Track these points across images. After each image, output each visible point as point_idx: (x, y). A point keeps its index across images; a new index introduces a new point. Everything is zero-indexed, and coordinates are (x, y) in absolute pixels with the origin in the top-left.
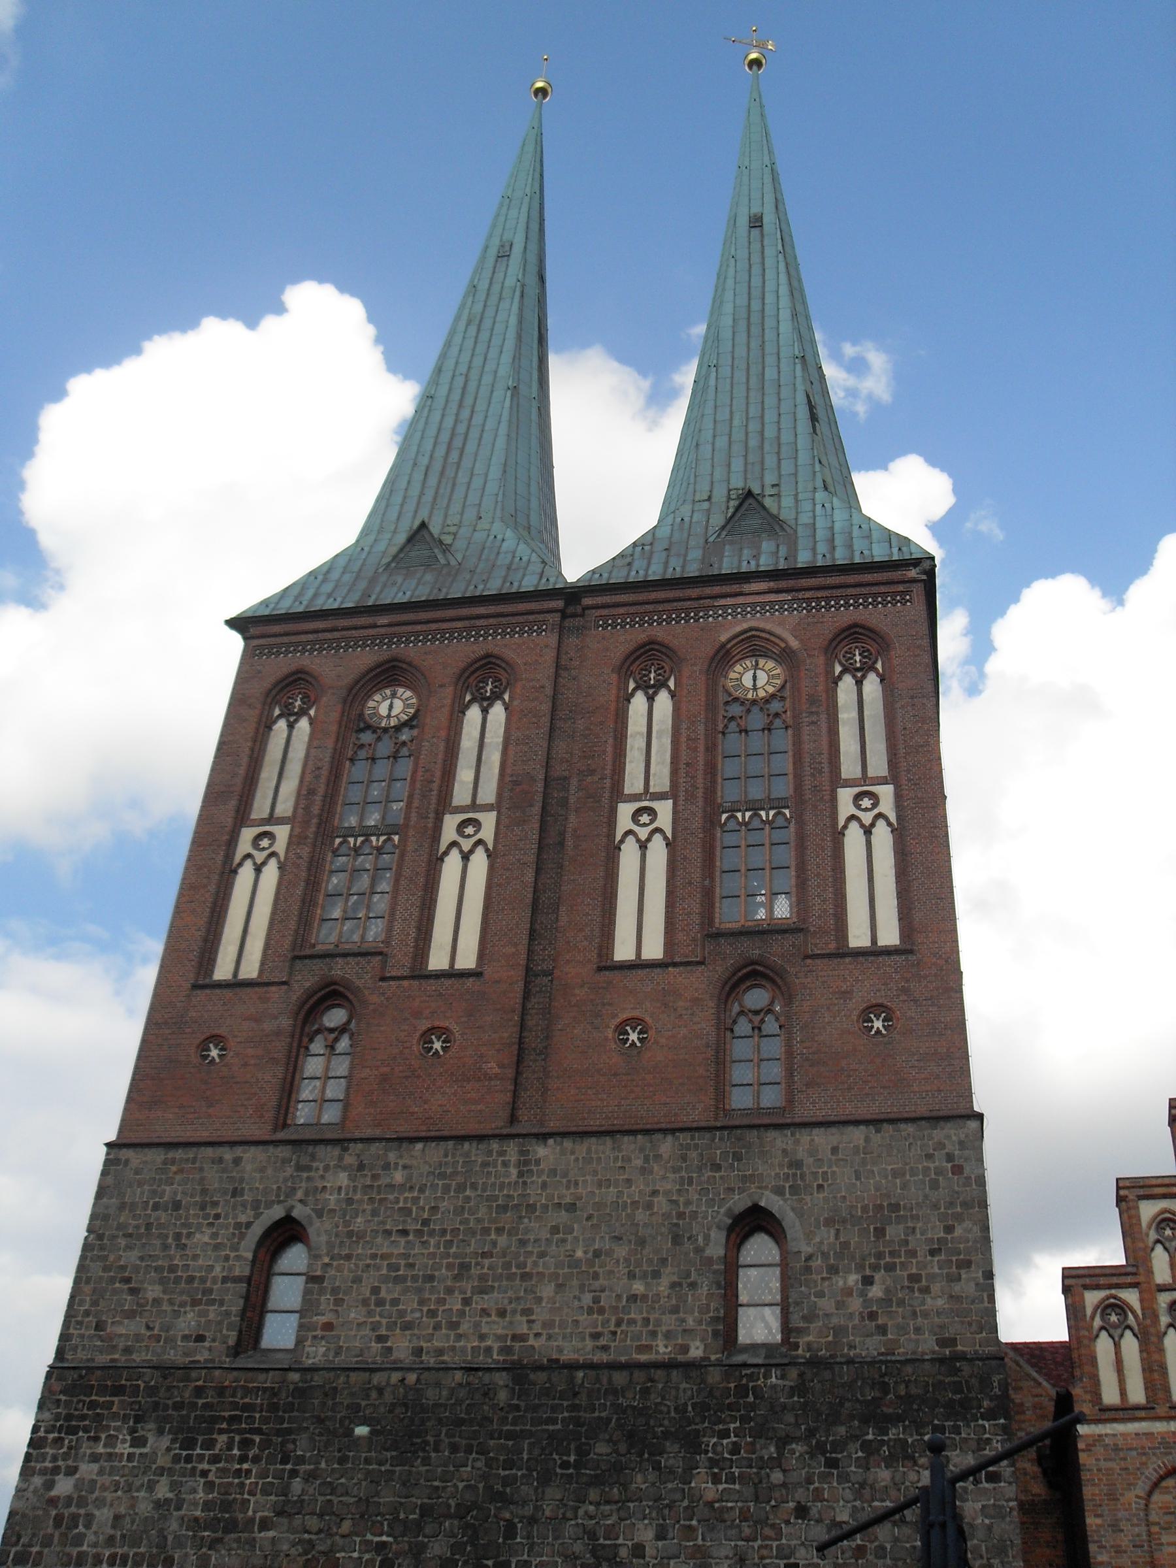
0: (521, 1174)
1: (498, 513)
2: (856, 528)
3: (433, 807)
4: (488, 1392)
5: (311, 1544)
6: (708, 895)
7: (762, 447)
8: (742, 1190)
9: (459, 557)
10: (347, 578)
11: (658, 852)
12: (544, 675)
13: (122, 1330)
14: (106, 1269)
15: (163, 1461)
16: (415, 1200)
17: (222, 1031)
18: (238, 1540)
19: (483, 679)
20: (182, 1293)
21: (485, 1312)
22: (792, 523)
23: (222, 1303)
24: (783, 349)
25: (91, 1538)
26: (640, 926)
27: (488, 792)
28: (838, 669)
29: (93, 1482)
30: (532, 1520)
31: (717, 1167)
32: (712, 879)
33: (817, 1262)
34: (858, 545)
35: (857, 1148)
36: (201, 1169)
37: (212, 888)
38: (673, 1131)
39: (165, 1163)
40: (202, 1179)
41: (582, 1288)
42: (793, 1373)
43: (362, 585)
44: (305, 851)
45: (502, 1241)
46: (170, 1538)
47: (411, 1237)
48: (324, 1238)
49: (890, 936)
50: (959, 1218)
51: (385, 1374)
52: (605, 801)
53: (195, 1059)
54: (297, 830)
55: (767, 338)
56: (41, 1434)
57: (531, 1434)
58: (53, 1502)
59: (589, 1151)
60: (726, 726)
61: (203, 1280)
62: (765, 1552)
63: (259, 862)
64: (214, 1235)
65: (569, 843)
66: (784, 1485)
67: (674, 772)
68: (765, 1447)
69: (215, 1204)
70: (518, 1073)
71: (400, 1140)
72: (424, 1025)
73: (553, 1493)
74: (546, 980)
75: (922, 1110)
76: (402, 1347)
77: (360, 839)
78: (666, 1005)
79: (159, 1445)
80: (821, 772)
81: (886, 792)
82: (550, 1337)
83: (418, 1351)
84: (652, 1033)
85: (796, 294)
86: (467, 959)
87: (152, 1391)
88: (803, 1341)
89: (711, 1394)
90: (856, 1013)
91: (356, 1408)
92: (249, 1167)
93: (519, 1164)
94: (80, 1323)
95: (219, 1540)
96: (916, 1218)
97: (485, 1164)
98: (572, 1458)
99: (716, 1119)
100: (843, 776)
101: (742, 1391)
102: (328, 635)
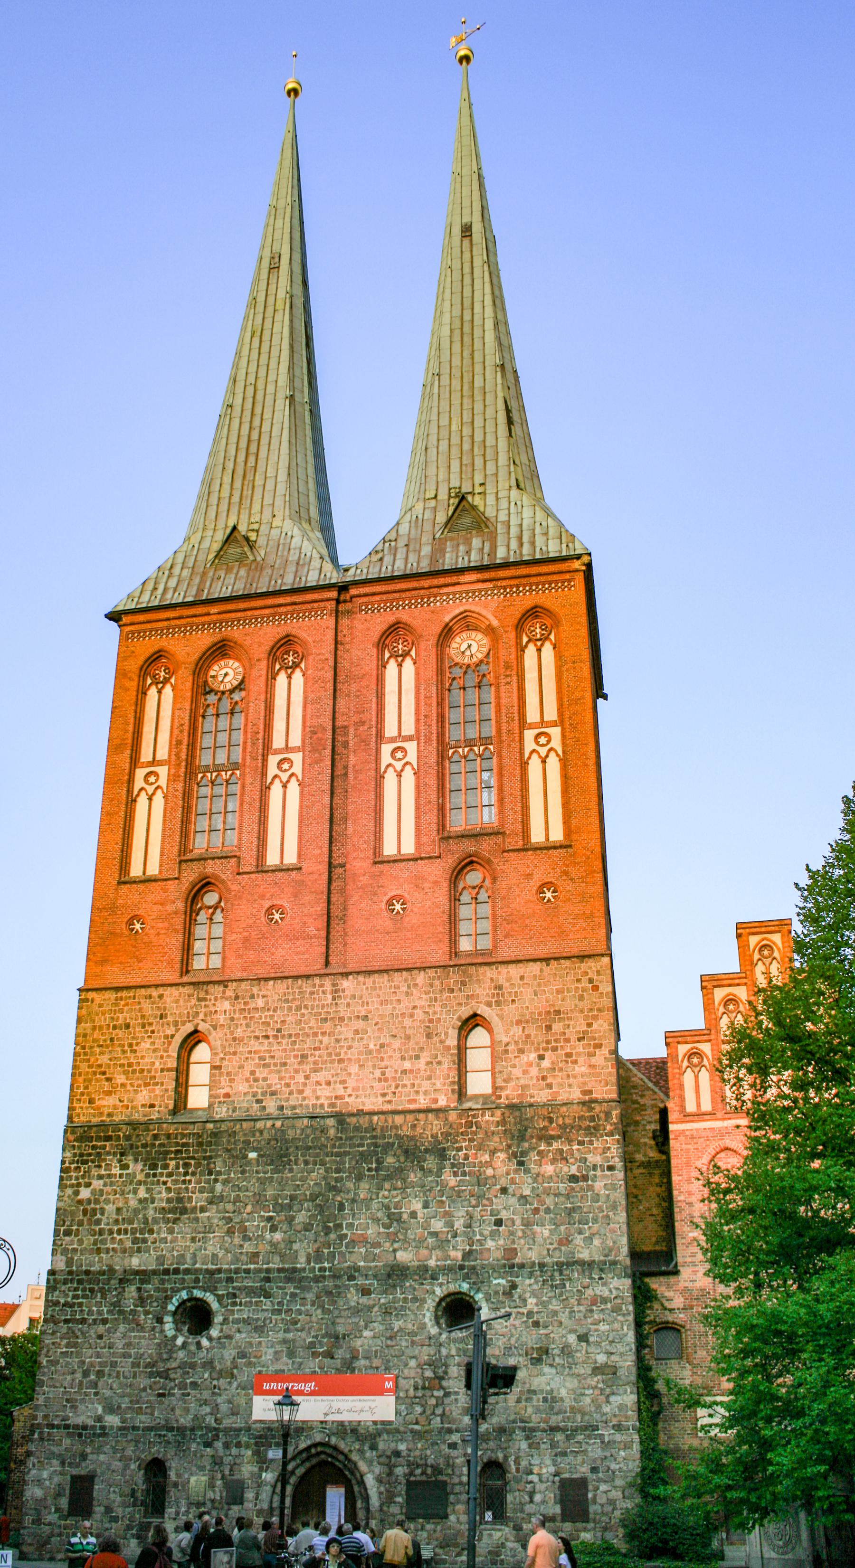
0: (334, 999)
1: (287, 513)
2: (538, 524)
3: (260, 751)
4: (324, 1130)
5: (230, 1220)
6: (442, 809)
7: (472, 450)
8: (467, 1004)
9: (262, 553)
10: (186, 573)
11: (409, 777)
13: (104, 1103)
14: (90, 1066)
15: (140, 1177)
16: (272, 1017)
17: (141, 912)
18: (189, 1218)
19: (285, 652)
20: (138, 1079)
21: (318, 1083)
22: (493, 520)
23: (162, 1084)
24: (487, 357)
25: (104, 1220)
26: (400, 833)
27: (296, 740)
28: (525, 639)
29: (101, 1191)
30: (354, 1201)
31: (452, 991)
32: (443, 796)
33: (511, 1047)
34: (540, 541)
35: (535, 976)
36: (139, 1003)
37: (122, 814)
38: (424, 969)
39: (116, 999)
40: (140, 1010)
41: (374, 1066)
42: (498, 1113)
43: (197, 580)
44: (180, 786)
45: (326, 1040)
46: (150, 1219)
47: (271, 1040)
48: (219, 1043)
49: (557, 835)
50: (595, 1018)
51: (263, 1122)
52: (373, 745)
53: (126, 932)
54: (173, 771)
55: (475, 348)
56: (67, 1165)
57: (348, 1153)
58: (80, 1202)
59: (374, 982)
60: (451, 685)
61: (149, 1071)
62: (484, 1213)
63: (150, 793)
64: (153, 1043)
65: (351, 775)
66: (494, 1176)
67: (417, 721)
68: (482, 1155)
69: (151, 1024)
70: (328, 933)
71: (259, 979)
72: (267, 904)
73: (364, 1185)
74: (341, 870)
75: (575, 951)
76: (271, 1106)
77: (215, 774)
78: (417, 886)
79: (136, 1168)
80: (513, 720)
81: (555, 732)
82: (357, 1097)
83: (281, 1108)
84: (409, 905)
85: (498, 302)
86: (291, 858)
87: (128, 1138)
88: (503, 1094)
89: (451, 1127)
90: (535, 888)
91: (247, 1142)
92: (168, 1000)
93: (332, 992)
94: (79, 1100)
95: (179, 1219)
96: (570, 1019)
97: (312, 993)
98: (374, 1166)
99: (450, 959)
100: (528, 721)
101: (470, 1124)
102: (178, 622)
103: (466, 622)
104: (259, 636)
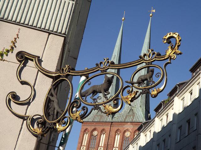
19: (103, 131)
27: (103, 146)
103: (127, 130)
104: (100, 128)
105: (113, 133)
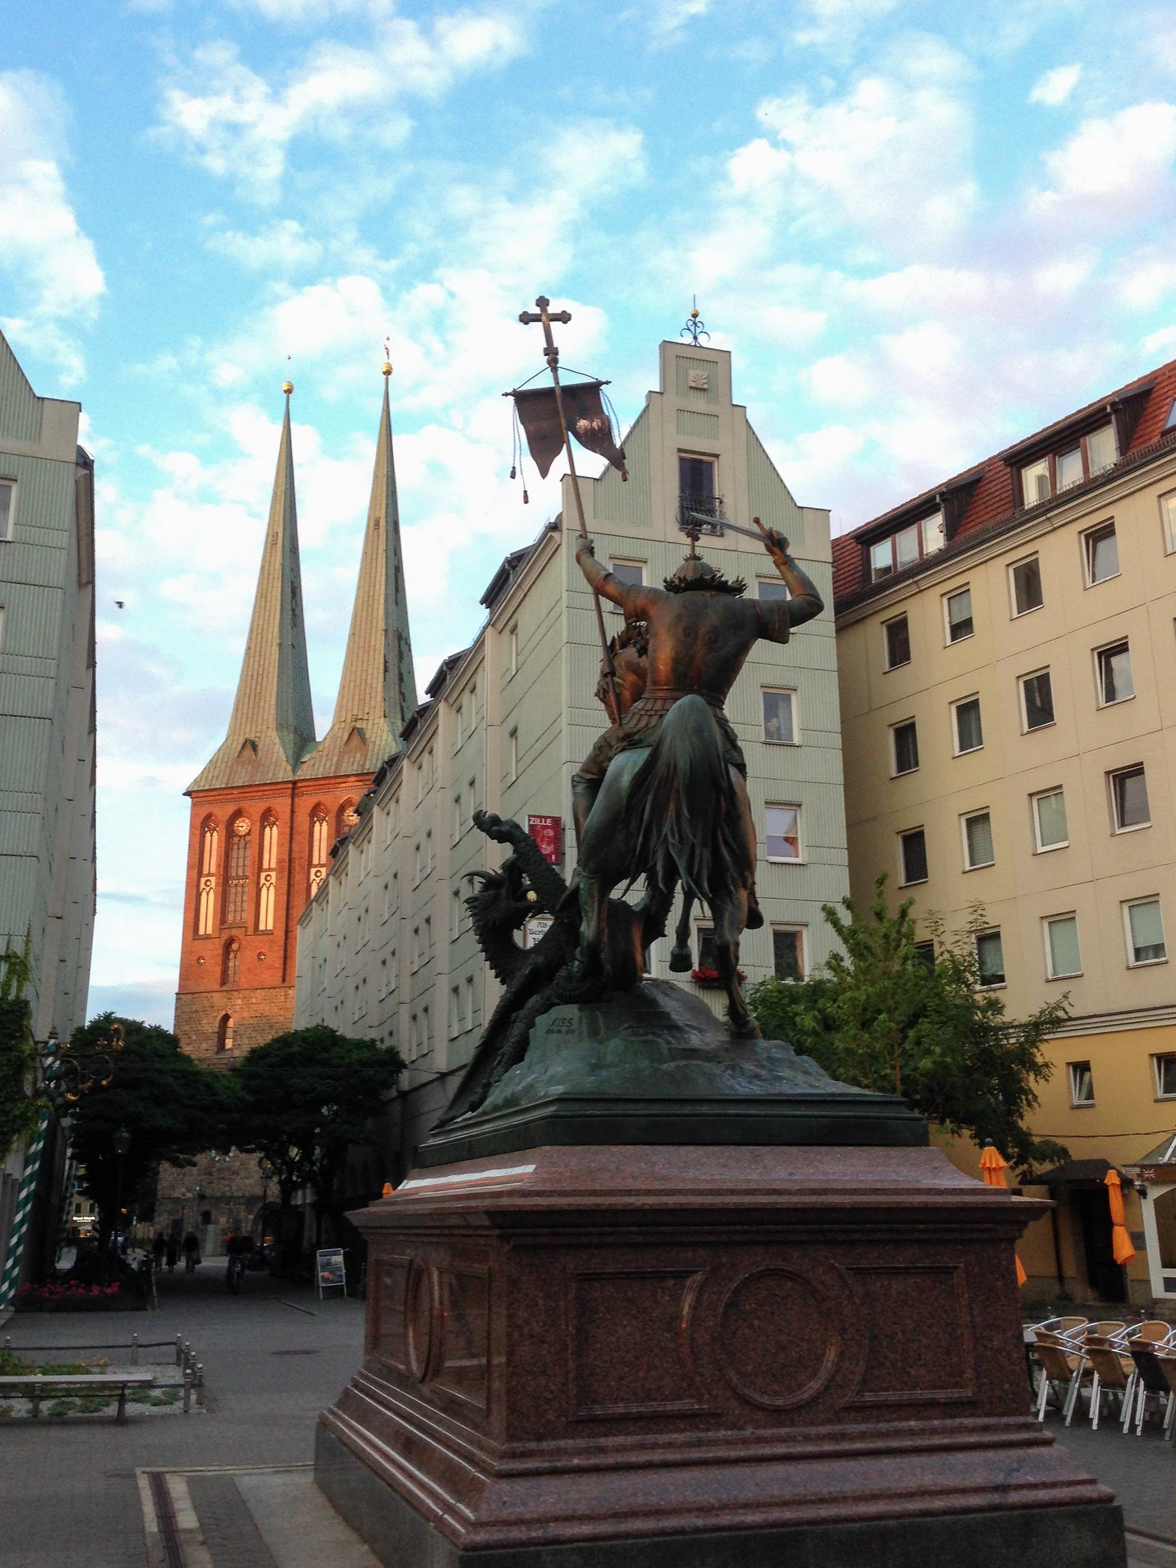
12: (287, 816)
19: (267, 818)
27: (273, 865)
86: (270, 927)
105: (302, 818)
